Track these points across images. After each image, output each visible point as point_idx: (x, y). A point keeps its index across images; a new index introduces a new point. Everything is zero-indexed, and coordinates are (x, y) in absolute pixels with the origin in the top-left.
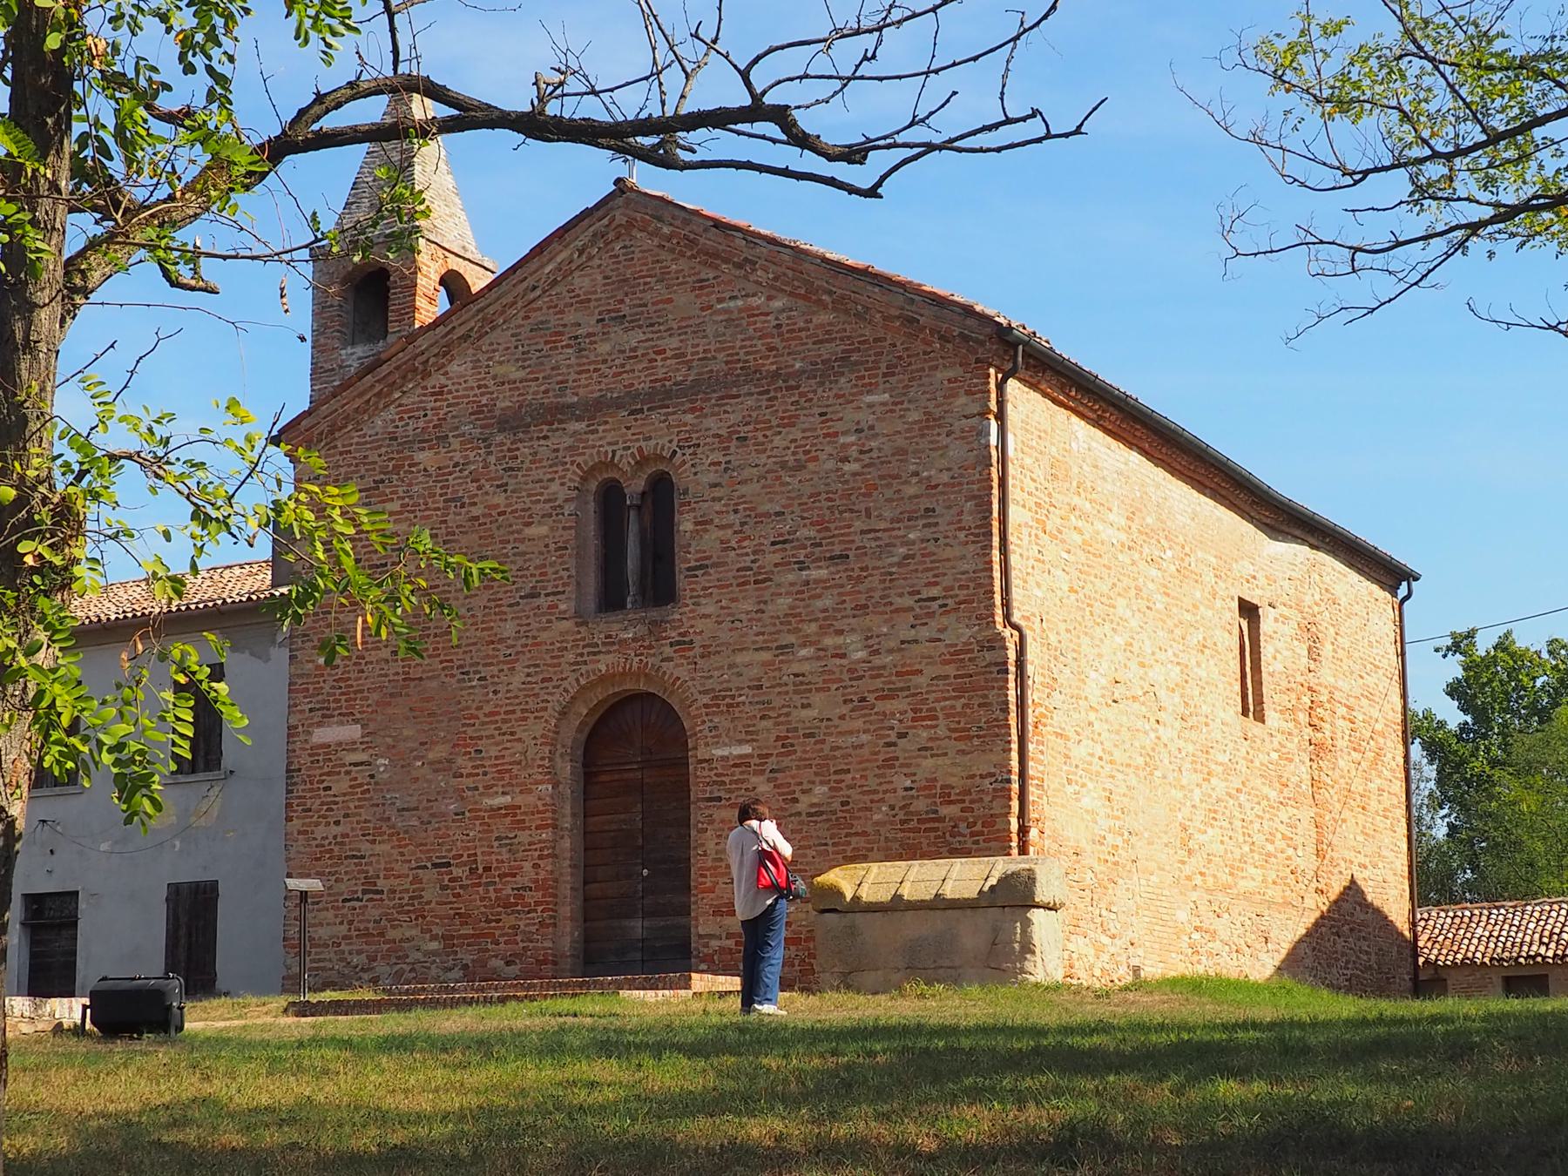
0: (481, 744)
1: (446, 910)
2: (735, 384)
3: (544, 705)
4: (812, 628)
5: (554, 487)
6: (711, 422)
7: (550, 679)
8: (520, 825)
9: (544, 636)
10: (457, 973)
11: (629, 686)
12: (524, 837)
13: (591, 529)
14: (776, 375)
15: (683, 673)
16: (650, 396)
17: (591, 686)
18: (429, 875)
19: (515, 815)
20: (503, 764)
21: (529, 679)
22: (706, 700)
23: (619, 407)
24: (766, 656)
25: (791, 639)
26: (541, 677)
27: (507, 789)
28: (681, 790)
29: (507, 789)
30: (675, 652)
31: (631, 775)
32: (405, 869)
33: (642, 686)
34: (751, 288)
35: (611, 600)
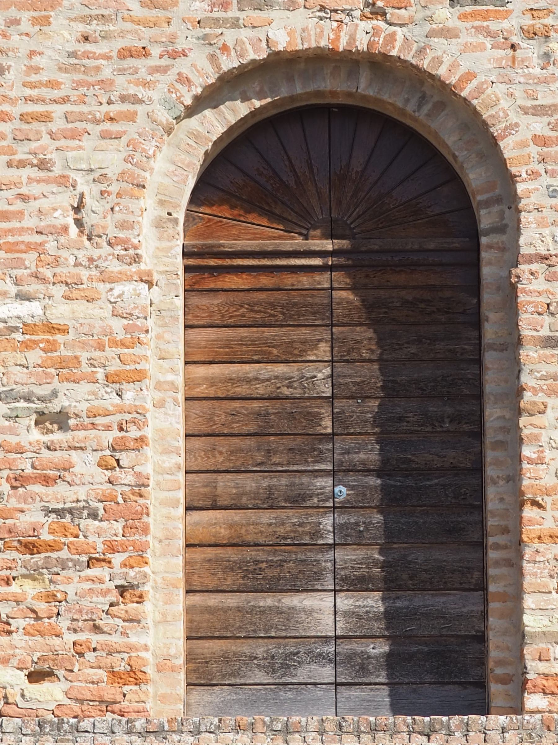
3: (126, 107)
7: (144, 52)
19: (51, 347)
20: (21, 231)
21: (88, 47)
26: (120, 44)
27: (33, 287)
29: (33, 287)
30: (463, 17)
31: (305, 280)
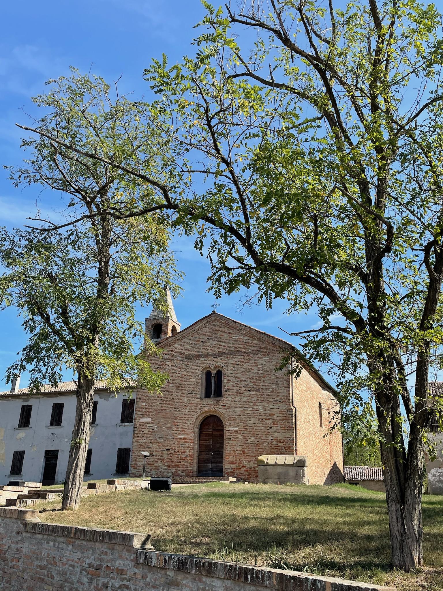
0: (178, 424)
1: (168, 460)
2: (236, 353)
4: (252, 404)
5: (197, 371)
6: (230, 361)
8: (186, 442)
9: (193, 402)
10: (170, 474)
11: (211, 414)
12: (187, 445)
13: (204, 380)
14: (245, 352)
15: (223, 412)
16: (218, 354)
17: (203, 413)
18: (165, 452)
22: (228, 418)
23: (212, 356)
24: (242, 409)
25: (247, 406)
28: (222, 436)
32: (160, 450)
33: (214, 414)
34: (240, 335)
35: (208, 395)
